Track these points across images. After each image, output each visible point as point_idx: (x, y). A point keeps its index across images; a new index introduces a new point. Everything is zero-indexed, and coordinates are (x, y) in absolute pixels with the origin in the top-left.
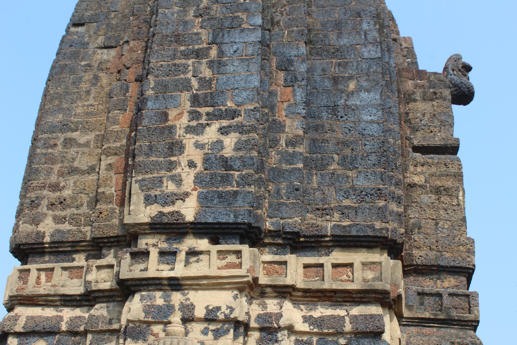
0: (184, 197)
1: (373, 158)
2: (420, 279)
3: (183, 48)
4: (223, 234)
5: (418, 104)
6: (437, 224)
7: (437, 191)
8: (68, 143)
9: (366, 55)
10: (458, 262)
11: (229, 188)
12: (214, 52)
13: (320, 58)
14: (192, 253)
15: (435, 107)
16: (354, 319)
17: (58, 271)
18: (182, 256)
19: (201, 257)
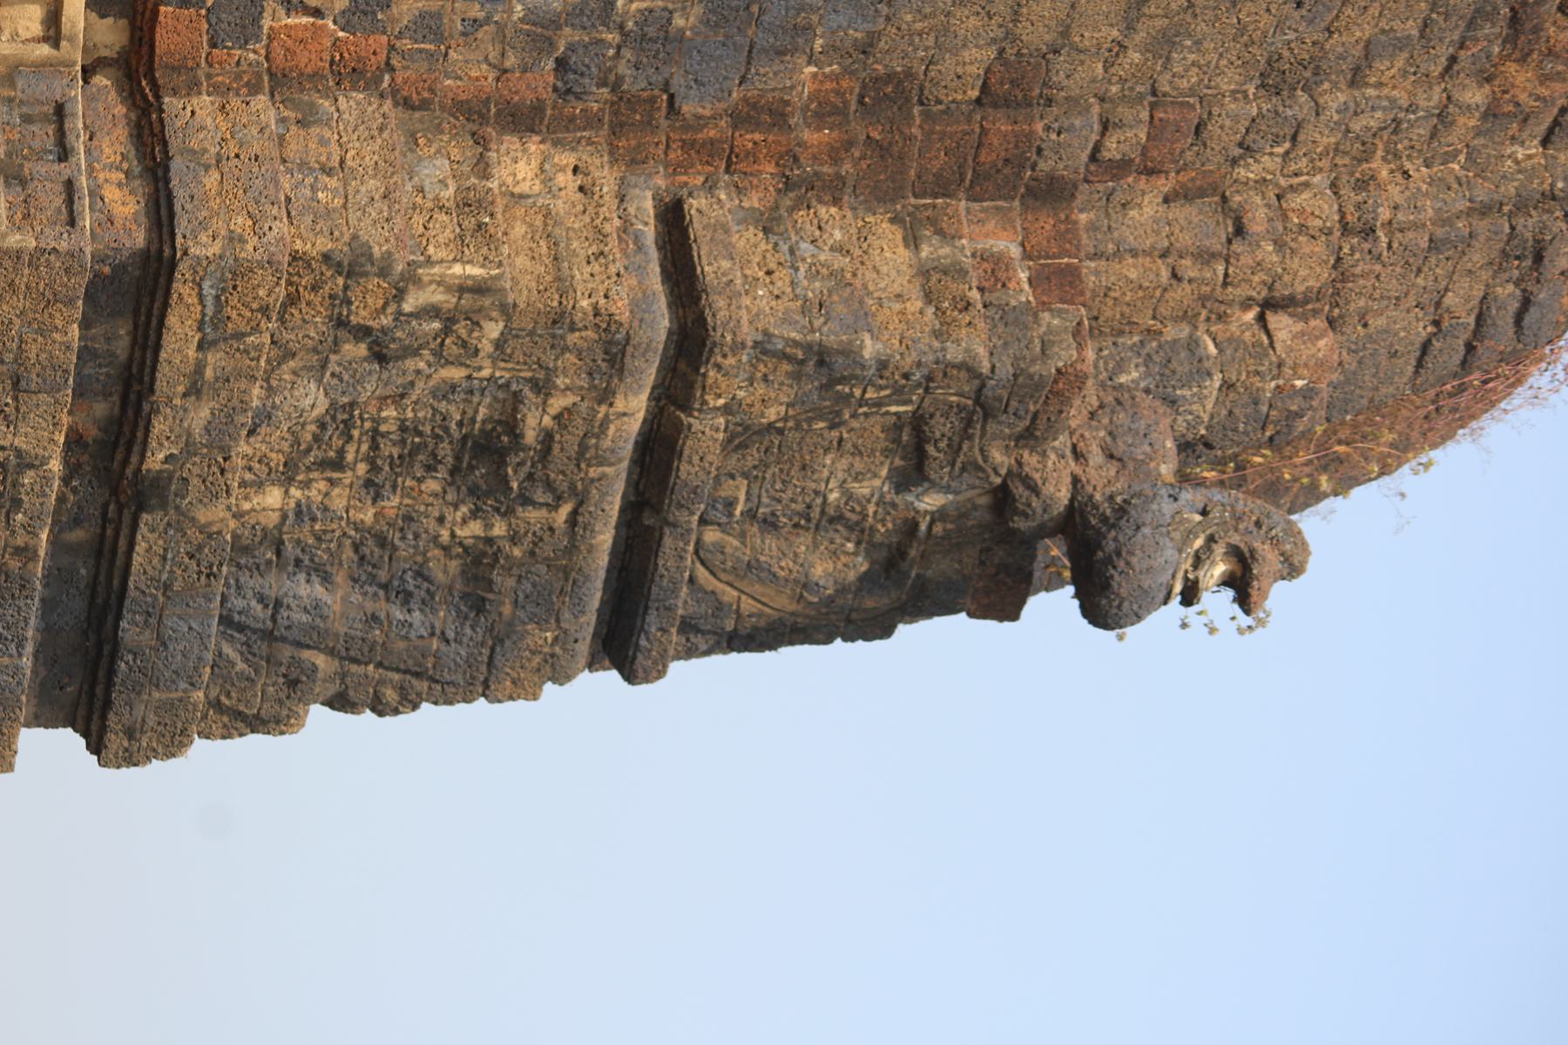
2: (122, 132)
5: (901, 250)
6: (329, 172)
7: (468, 204)
10: (188, 206)
15: (897, 307)
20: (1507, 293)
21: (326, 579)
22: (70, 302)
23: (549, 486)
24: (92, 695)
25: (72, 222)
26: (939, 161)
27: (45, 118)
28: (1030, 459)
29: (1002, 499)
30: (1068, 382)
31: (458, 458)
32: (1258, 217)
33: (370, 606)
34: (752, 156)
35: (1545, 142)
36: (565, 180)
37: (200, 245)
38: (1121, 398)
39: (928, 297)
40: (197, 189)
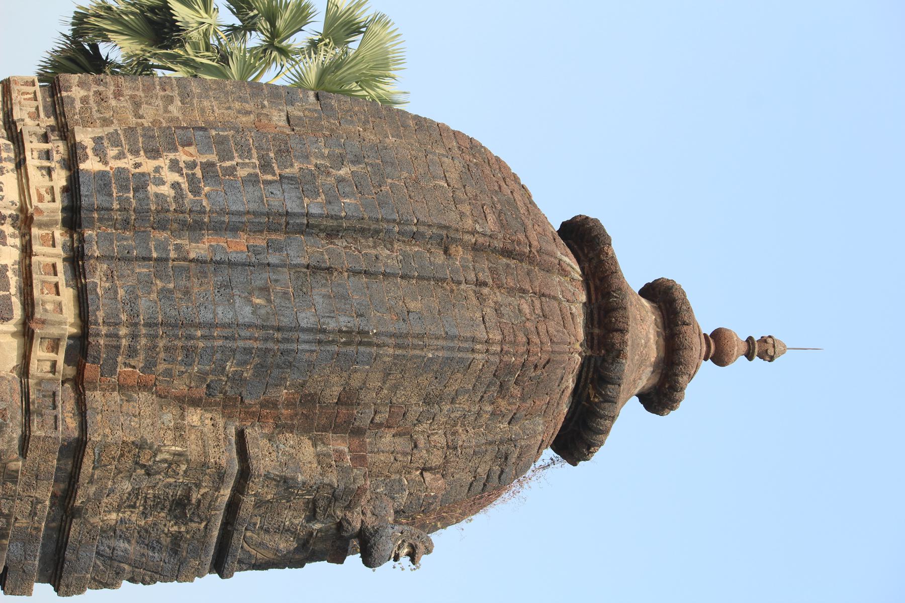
0: (104, 161)
1: (174, 313)
2: (73, 401)
3: (272, 155)
4: (72, 195)
6: (135, 416)
7: (176, 428)
8: (169, 100)
9: (301, 315)
11: (115, 191)
12: (269, 177)
13: (293, 277)
14: (49, 171)
16: (8, 298)
17: (35, 103)
18: (46, 163)
19: (47, 177)
20: (496, 468)
21: (129, 542)
22: (54, 453)
23: (199, 516)
24: (56, 574)
25: (56, 428)
26: (324, 421)
27: (50, 396)
28: (349, 514)
29: (340, 526)
30: (361, 491)
31: (171, 507)
32: (422, 443)
33: (142, 551)
34: (266, 417)
35: (509, 423)
36: (208, 421)
37: (94, 437)
38: (378, 496)
39: (319, 463)
40: (95, 420)
